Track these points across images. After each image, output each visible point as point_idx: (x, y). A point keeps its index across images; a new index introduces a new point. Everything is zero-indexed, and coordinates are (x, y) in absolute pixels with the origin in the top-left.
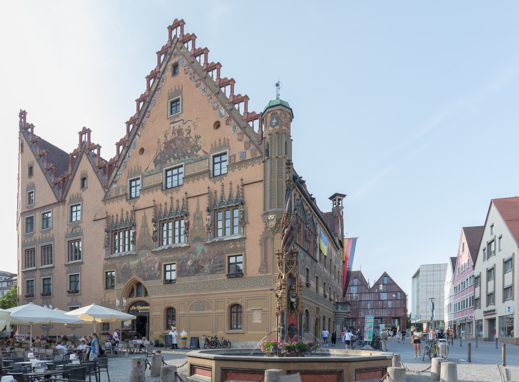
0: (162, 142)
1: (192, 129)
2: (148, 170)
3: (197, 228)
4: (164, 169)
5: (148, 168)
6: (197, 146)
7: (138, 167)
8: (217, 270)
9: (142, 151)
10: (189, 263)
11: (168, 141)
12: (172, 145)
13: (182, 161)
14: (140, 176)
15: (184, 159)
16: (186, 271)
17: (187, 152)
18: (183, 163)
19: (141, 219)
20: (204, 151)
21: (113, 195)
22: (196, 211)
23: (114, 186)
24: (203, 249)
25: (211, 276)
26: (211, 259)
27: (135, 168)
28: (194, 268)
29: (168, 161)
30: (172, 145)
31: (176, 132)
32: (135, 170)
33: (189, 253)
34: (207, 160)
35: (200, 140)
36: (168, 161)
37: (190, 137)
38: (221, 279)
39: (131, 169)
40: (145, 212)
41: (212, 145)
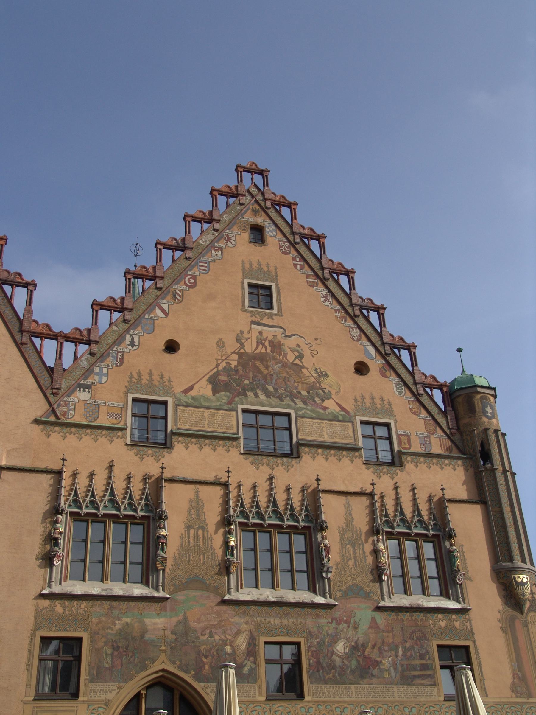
0: (229, 350)
1: (307, 352)
2: (193, 393)
3: (351, 563)
4: (240, 407)
5: (191, 388)
6: (323, 389)
7: (162, 377)
8: (415, 677)
9: (171, 347)
10: (340, 647)
11: (247, 354)
12: (258, 363)
13: (289, 407)
15: (292, 404)
16: (334, 668)
17: (299, 392)
18: (292, 412)
19: (185, 506)
20: (340, 406)
22: (347, 524)
23: (83, 396)
24: (373, 620)
25: (403, 688)
26: (397, 647)
27: (151, 374)
28: (354, 664)
29: (250, 394)
30: (258, 363)
31: (267, 344)
32: (151, 380)
33: (339, 622)
34: (350, 425)
35: (327, 381)
36: (250, 394)
37: (303, 367)
38: (429, 699)
39: (139, 374)
40: (197, 492)
41: (356, 400)
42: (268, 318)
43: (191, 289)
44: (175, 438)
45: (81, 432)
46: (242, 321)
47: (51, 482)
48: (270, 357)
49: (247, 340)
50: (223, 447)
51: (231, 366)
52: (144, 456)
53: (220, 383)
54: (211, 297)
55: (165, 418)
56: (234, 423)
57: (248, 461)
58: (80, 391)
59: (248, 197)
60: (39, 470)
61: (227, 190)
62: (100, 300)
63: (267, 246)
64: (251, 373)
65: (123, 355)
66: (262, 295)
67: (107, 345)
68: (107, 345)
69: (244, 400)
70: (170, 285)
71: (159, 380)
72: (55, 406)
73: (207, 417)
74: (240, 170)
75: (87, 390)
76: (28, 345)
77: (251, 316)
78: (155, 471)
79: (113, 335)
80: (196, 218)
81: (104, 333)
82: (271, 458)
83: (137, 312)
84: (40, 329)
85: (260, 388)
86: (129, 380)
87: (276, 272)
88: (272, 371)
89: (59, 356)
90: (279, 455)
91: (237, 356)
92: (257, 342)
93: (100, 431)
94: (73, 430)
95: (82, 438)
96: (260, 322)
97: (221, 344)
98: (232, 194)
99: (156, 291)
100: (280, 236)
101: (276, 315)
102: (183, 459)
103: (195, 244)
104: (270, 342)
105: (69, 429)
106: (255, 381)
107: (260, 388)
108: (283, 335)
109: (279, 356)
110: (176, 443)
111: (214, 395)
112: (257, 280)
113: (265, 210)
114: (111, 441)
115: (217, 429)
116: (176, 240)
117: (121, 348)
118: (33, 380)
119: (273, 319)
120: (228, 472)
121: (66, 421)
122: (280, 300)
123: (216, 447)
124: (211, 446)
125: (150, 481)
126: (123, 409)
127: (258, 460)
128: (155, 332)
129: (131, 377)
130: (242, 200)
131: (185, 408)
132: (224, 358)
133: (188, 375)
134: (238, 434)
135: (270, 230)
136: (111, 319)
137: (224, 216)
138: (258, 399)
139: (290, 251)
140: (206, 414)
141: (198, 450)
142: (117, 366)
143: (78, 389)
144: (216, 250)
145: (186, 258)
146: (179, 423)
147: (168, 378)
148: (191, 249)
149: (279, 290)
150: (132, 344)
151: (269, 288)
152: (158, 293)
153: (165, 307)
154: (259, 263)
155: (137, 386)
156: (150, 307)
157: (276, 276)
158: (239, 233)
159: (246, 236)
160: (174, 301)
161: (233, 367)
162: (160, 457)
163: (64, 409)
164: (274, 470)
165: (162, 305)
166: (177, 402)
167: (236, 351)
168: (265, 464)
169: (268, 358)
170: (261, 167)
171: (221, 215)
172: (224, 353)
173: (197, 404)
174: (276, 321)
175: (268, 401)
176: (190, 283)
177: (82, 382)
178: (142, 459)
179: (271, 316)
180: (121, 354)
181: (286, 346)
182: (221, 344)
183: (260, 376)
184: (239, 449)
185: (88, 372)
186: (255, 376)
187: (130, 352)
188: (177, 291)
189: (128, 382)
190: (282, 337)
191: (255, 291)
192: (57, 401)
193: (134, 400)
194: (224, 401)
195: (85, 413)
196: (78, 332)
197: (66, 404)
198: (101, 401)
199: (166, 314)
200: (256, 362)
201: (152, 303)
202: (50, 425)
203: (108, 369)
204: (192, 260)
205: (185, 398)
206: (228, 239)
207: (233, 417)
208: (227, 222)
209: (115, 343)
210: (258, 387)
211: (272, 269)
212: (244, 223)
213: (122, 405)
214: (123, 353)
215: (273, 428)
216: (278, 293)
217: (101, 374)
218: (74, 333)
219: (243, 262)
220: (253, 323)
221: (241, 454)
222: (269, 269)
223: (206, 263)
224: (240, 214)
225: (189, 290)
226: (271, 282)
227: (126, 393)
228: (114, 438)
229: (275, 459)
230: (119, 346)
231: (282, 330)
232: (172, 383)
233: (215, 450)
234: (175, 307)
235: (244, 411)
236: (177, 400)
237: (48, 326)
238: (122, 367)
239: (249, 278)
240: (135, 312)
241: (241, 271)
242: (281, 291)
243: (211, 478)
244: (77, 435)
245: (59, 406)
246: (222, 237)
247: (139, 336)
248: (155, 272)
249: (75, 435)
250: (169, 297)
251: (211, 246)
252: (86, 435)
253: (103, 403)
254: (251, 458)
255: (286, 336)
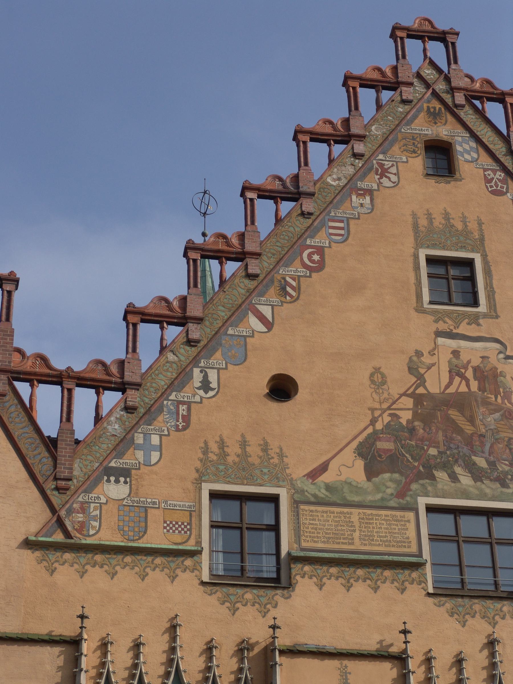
2: (327, 478)
4: (422, 502)
5: (324, 468)
7: (265, 448)
9: (282, 389)
11: (429, 396)
12: (453, 413)
14: (284, 494)
21: (108, 536)
23: (115, 490)
27: (244, 444)
29: (441, 475)
30: (453, 413)
31: (469, 374)
32: (244, 455)
36: (441, 475)
39: (222, 444)
42: (468, 324)
43: (314, 275)
44: (296, 568)
45: (114, 562)
46: (418, 331)
47: (60, 661)
48: (476, 401)
49: (429, 368)
50: (392, 583)
51: (401, 420)
52: (238, 605)
53: (380, 456)
54: (354, 287)
55: (276, 528)
56: (412, 533)
57: (442, 609)
58: (108, 481)
59: (419, 87)
60: (36, 638)
61: (376, 76)
62: (141, 303)
63: (460, 180)
64: (440, 433)
65: (189, 409)
66: (454, 278)
67: (157, 390)
68: (157, 390)
69: (429, 488)
70: (274, 267)
71: (261, 454)
72: (63, 513)
73: (357, 524)
74: (399, 34)
75: (122, 479)
76: (7, 398)
77: (436, 321)
78: (259, 634)
79: (167, 370)
80: (317, 134)
81: (150, 367)
82: (489, 602)
83: (211, 324)
84: (28, 366)
85: (460, 462)
86: (201, 456)
87: (481, 230)
88: (482, 427)
89: (67, 415)
90: (505, 595)
91: (411, 400)
92: (450, 372)
93: (150, 559)
94: (99, 558)
95: (116, 573)
96: (455, 331)
97: (377, 378)
98: (386, 82)
99: (247, 281)
100: (486, 160)
101: (485, 316)
102: (315, 609)
103: (318, 185)
104: (476, 369)
105: (90, 556)
106: (449, 448)
107: (460, 462)
108: (502, 356)
109: (496, 398)
110: (298, 578)
111: (369, 479)
112: (444, 248)
113: (452, 110)
114: (173, 578)
115: (378, 547)
116: (280, 179)
117: (185, 395)
118: (19, 464)
119: (479, 325)
120: (405, 632)
121: (84, 542)
122: (492, 287)
123: (379, 583)
124: (368, 582)
125: (251, 654)
126: (194, 513)
127: (464, 606)
128: (248, 360)
129: (206, 450)
130: (407, 93)
131: (312, 508)
132: (385, 406)
133: (316, 444)
134: (420, 555)
135: (464, 150)
136: (162, 339)
137: (373, 128)
138: (458, 485)
139: (507, 188)
140: (355, 519)
141: (343, 590)
142: (178, 430)
143: (106, 478)
144: (360, 195)
145: (303, 214)
146: (303, 538)
147: (278, 451)
148: (311, 195)
149: (489, 267)
150: (206, 386)
151: (469, 263)
152: (251, 284)
153: (266, 311)
154: (447, 216)
155: (217, 469)
156: (238, 312)
157: (482, 239)
158: (404, 159)
159: (418, 163)
160: (283, 299)
161: (404, 423)
162: (269, 606)
163: (80, 517)
164: (497, 627)
165: (261, 308)
166: (297, 497)
167: (409, 392)
168: (478, 615)
169: (474, 403)
170: (441, 25)
171: (367, 127)
172: (385, 395)
173: (336, 498)
174: (486, 328)
175: (477, 489)
176: (313, 262)
177: (113, 464)
178: (234, 611)
179: (475, 320)
180: (185, 407)
181: (508, 377)
182: (377, 378)
183: (459, 438)
184: (423, 585)
185: (124, 444)
186: (449, 440)
187: (201, 402)
188: (288, 279)
189: (201, 460)
190: (498, 360)
191: (440, 270)
192: (67, 502)
193: (214, 495)
194: (389, 491)
195: (121, 524)
196: (100, 367)
197: (83, 510)
198: (149, 500)
199: (269, 325)
200: (450, 412)
201: (240, 306)
202: (55, 550)
203: (161, 436)
204: (313, 217)
205: (312, 487)
206: (383, 173)
207: (409, 521)
208: (380, 139)
209: (172, 386)
210: (456, 461)
211: (473, 226)
212: (414, 139)
213: (190, 507)
214: (189, 404)
215: (490, 542)
216: (488, 272)
217: (147, 448)
218: (93, 371)
219: (414, 215)
220: (439, 334)
221: (429, 595)
222: (466, 226)
223: (342, 221)
224: (404, 122)
225: (310, 276)
226: (473, 251)
227: (198, 482)
228: (178, 571)
229: (498, 605)
230: (180, 391)
231: (498, 346)
232: (285, 459)
233: (376, 589)
234: (286, 310)
235: (430, 509)
236: (297, 492)
237: (43, 359)
238: (187, 431)
239: (428, 247)
240: (207, 323)
241: (411, 233)
242: (492, 268)
243: (371, 645)
244: (106, 567)
245: (70, 512)
246: (370, 169)
247: (219, 369)
248: (243, 245)
249: (102, 567)
250: (272, 291)
251: (350, 187)
252: (124, 568)
253: (155, 503)
254: (449, 604)
255: (508, 357)
